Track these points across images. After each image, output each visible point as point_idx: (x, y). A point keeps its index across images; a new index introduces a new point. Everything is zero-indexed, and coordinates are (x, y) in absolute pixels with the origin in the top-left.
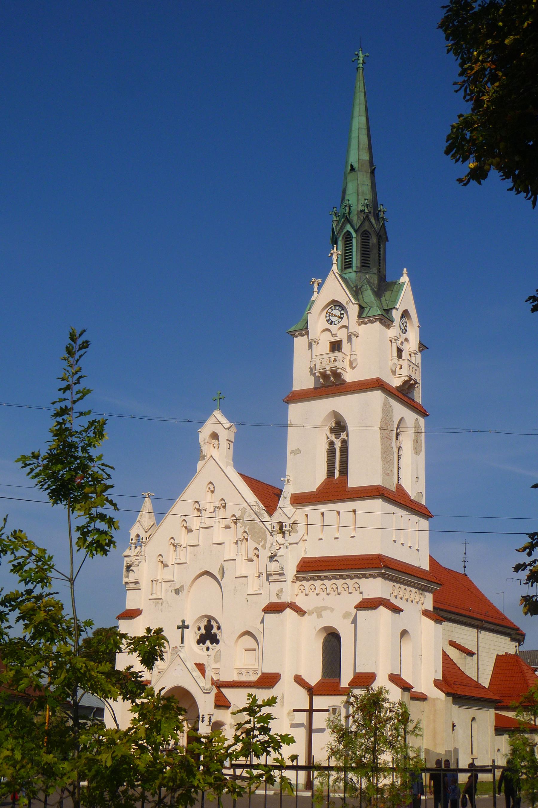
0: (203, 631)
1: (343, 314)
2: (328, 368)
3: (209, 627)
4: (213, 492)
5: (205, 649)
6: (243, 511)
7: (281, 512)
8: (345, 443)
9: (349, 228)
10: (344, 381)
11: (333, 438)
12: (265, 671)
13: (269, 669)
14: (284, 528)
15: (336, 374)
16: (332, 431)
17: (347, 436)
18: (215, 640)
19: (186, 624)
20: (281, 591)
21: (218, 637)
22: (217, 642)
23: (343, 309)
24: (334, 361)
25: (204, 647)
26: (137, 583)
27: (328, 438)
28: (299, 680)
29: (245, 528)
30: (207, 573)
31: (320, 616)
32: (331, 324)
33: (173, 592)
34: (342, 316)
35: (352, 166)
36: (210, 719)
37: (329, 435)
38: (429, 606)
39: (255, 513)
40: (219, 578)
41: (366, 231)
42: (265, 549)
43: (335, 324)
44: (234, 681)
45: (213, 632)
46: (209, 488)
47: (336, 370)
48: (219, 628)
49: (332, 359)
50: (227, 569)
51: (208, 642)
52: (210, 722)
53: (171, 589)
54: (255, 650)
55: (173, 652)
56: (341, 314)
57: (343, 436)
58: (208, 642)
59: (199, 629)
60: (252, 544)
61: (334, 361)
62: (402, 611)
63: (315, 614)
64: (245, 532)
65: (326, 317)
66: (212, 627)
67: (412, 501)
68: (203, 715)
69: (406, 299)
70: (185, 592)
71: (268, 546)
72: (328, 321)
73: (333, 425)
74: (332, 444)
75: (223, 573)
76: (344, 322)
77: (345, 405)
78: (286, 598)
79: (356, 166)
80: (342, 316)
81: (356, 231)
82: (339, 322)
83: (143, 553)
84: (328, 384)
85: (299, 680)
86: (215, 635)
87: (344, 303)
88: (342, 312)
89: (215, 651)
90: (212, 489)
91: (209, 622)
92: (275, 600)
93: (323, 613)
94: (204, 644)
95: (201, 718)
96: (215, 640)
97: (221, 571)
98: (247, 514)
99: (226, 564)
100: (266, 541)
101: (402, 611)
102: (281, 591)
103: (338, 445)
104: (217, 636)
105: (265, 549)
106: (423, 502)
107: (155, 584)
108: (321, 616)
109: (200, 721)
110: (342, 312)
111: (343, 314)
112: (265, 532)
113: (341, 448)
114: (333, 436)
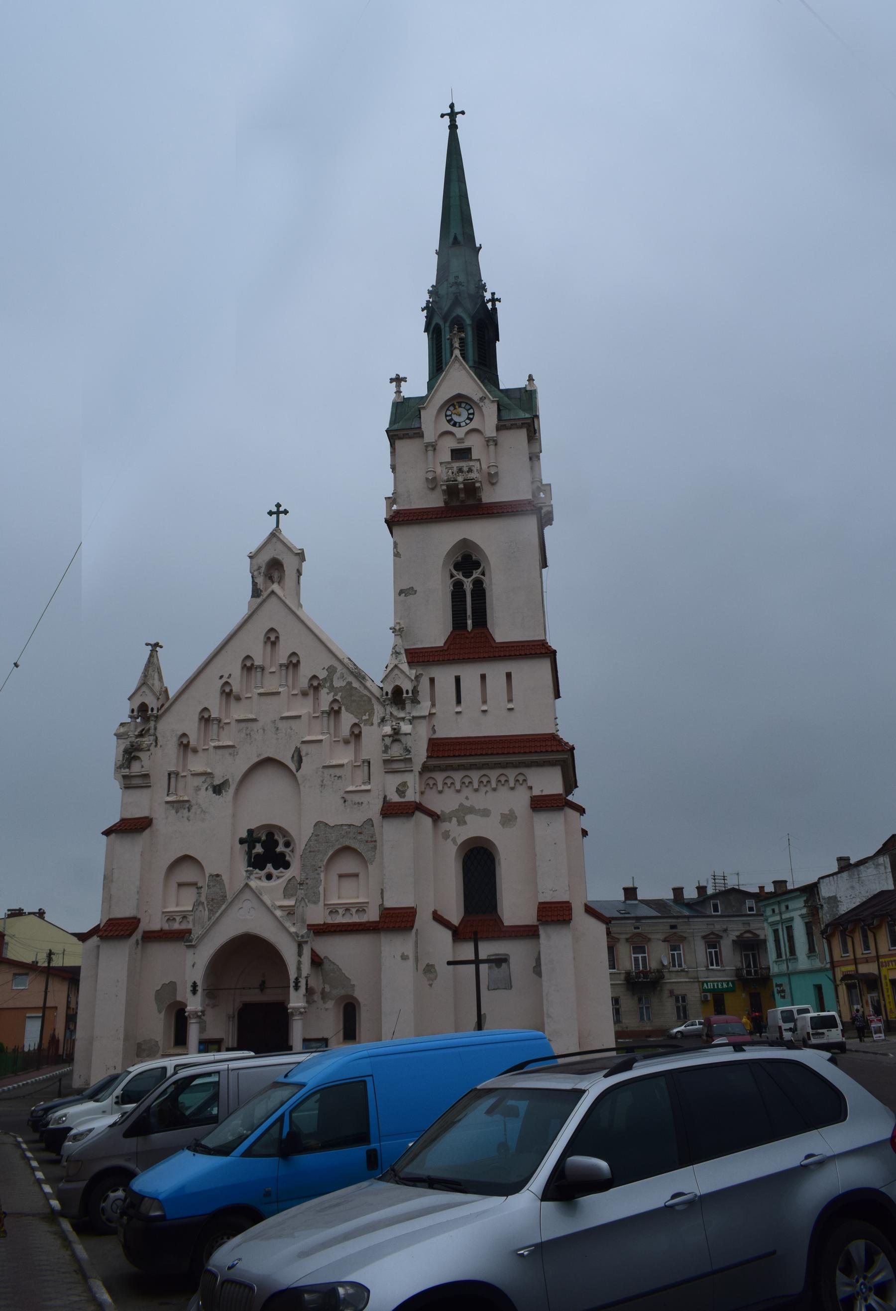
1: (473, 414)
4: (274, 644)
5: (264, 878)
6: (331, 670)
7: (399, 673)
8: (478, 583)
9: (459, 311)
10: (480, 500)
11: (459, 576)
12: (389, 904)
13: (396, 900)
14: (405, 695)
15: (472, 489)
16: (457, 566)
17: (483, 574)
18: (282, 863)
19: (255, 835)
20: (404, 784)
21: (287, 858)
22: (287, 865)
23: (472, 408)
24: (468, 472)
25: (263, 873)
26: (146, 776)
27: (452, 576)
28: (438, 918)
29: (335, 695)
30: (269, 761)
31: (462, 822)
32: (454, 425)
33: (210, 790)
34: (471, 416)
35: (455, 238)
36: (307, 984)
37: (455, 572)
39: (352, 673)
40: (293, 767)
42: (372, 724)
43: (460, 426)
44: (325, 924)
45: (278, 850)
46: (269, 638)
47: (474, 483)
48: (287, 844)
49: (465, 469)
50: (307, 754)
51: (269, 866)
52: (307, 989)
53: (206, 785)
54: (356, 875)
55: (211, 884)
56: (469, 414)
57: (476, 574)
58: (269, 866)
60: (347, 719)
61: (468, 472)
63: (454, 820)
64: (335, 701)
65: (446, 416)
66: (276, 844)
68: (297, 979)
70: (231, 790)
71: (376, 720)
72: (449, 421)
73: (460, 559)
74: (458, 586)
75: (300, 761)
76: (473, 425)
77: (480, 533)
78: (411, 796)
79: (460, 238)
80: (471, 416)
81: (473, 318)
82: (467, 424)
83: (152, 731)
84: (455, 503)
85: (438, 918)
86: (283, 855)
87: (476, 398)
88: (471, 411)
90: (273, 639)
91: (270, 835)
92: (395, 798)
93: (468, 818)
94: (262, 868)
95: (292, 984)
97: (295, 758)
98: (338, 675)
99: (304, 749)
100: (371, 714)
102: (404, 784)
104: (285, 856)
105: (372, 724)
107: (173, 780)
108: (465, 823)
109: (292, 989)
110: (471, 411)
111: (473, 414)
112: (370, 700)
113: (472, 591)
114: (461, 573)
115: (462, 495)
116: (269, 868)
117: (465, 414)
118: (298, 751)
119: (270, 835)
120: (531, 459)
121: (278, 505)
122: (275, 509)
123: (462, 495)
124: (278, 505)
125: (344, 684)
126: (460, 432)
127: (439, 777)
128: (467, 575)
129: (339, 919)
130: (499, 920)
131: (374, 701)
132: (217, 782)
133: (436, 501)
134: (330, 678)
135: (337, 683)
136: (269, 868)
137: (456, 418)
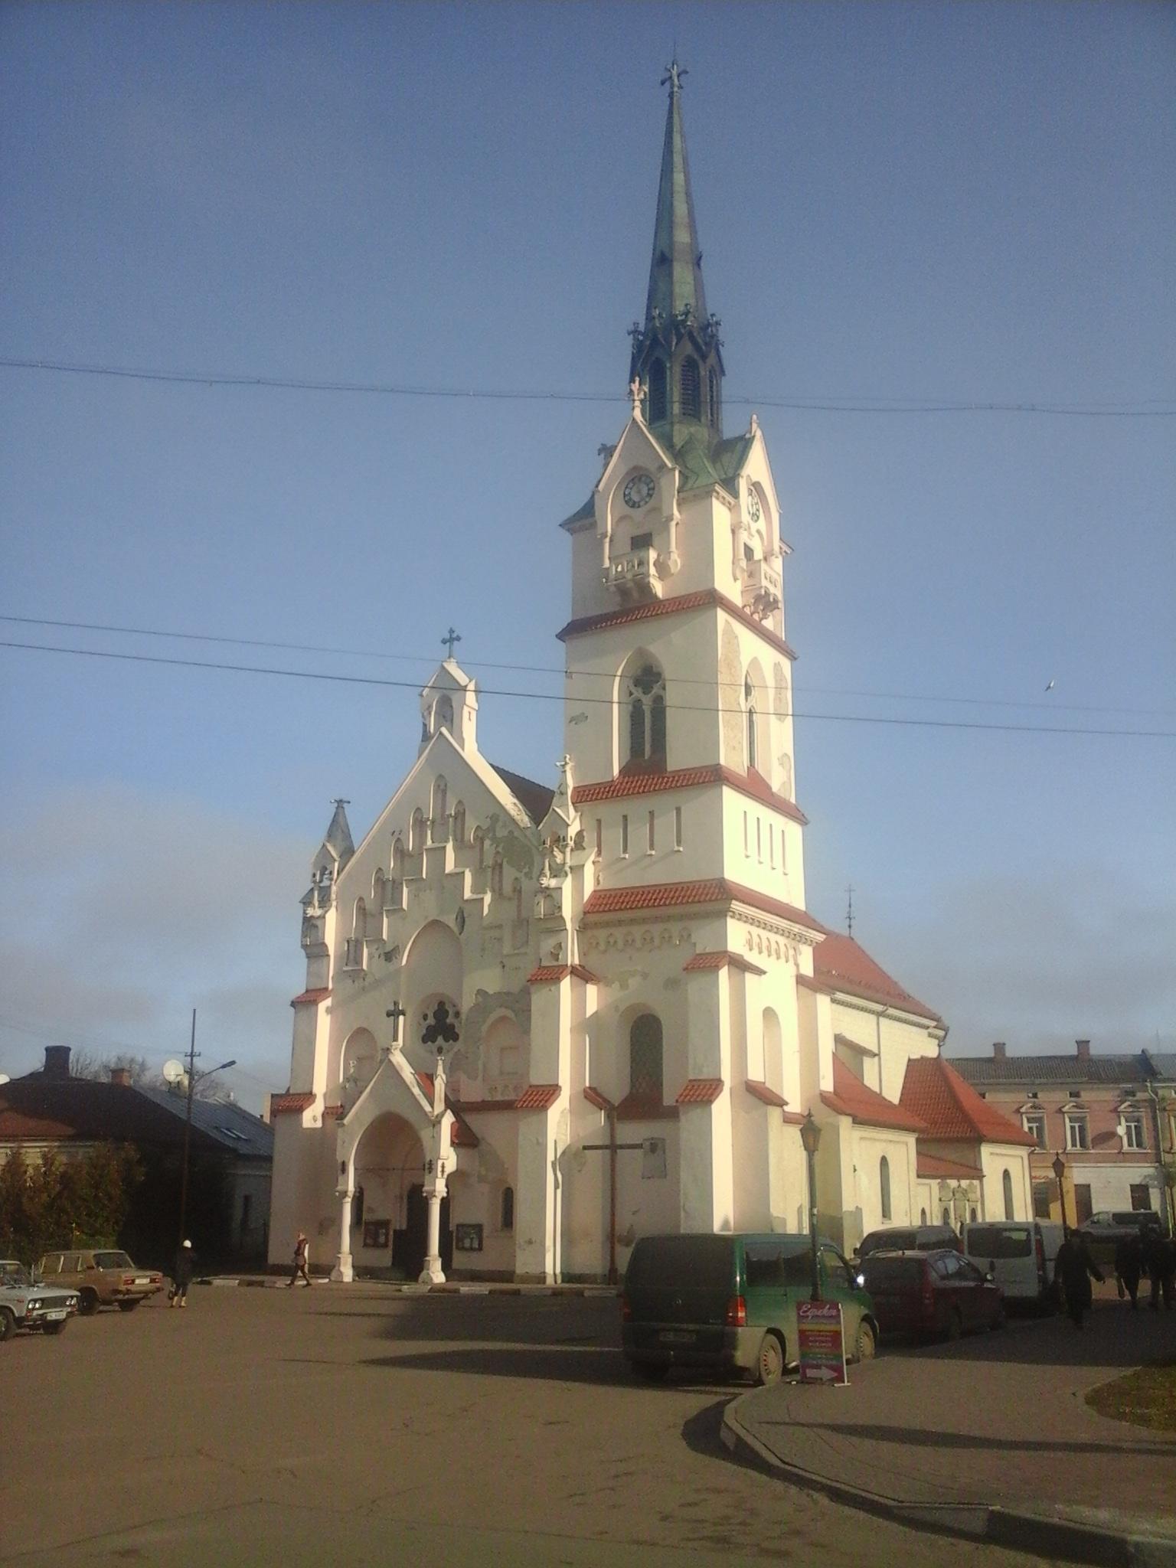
0: (431, 1021)
2: (629, 576)
3: (441, 1012)
8: (659, 700)
11: (638, 693)
16: (637, 683)
18: (451, 1034)
22: (456, 1038)
25: (433, 1047)
27: (631, 694)
32: (633, 506)
38: (808, 969)
41: (689, 357)
45: (448, 1021)
48: (457, 1014)
51: (440, 1039)
57: (656, 690)
58: (440, 1039)
59: (425, 1017)
60: (509, 873)
62: (765, 973)
67: (773, 794)
69: (756, 466)
71: (536, 872)
76: (652, 502)
86: (453, 1026)
89: (451, 1055)
91: (441, 1004)
96: (451, 1034)
98: (500, 824)
100: (531, 864)
101: (765, 973)
103: (647, 701)
106: (793, 800)
115: (635, 595)
116: (440, 1040)
117: (645, 491)
118: (461, 912)
119: (441, 1004)
120: (733, 532)
121: (452, 631)
122: (447, 636)
123: (635, 595)
124: (452, 631)
125: (506, 833)
126: (637, 514)
127: (602, 934)
128: (646, 691)
129: (499, 1098)
130: (660, 1098)
131: (534, 851)
132: (389, 948)
133: (611, 605)
134: (492, 829)
135: (501, 833)
136: (440, 1040)
137: (635, 498)
